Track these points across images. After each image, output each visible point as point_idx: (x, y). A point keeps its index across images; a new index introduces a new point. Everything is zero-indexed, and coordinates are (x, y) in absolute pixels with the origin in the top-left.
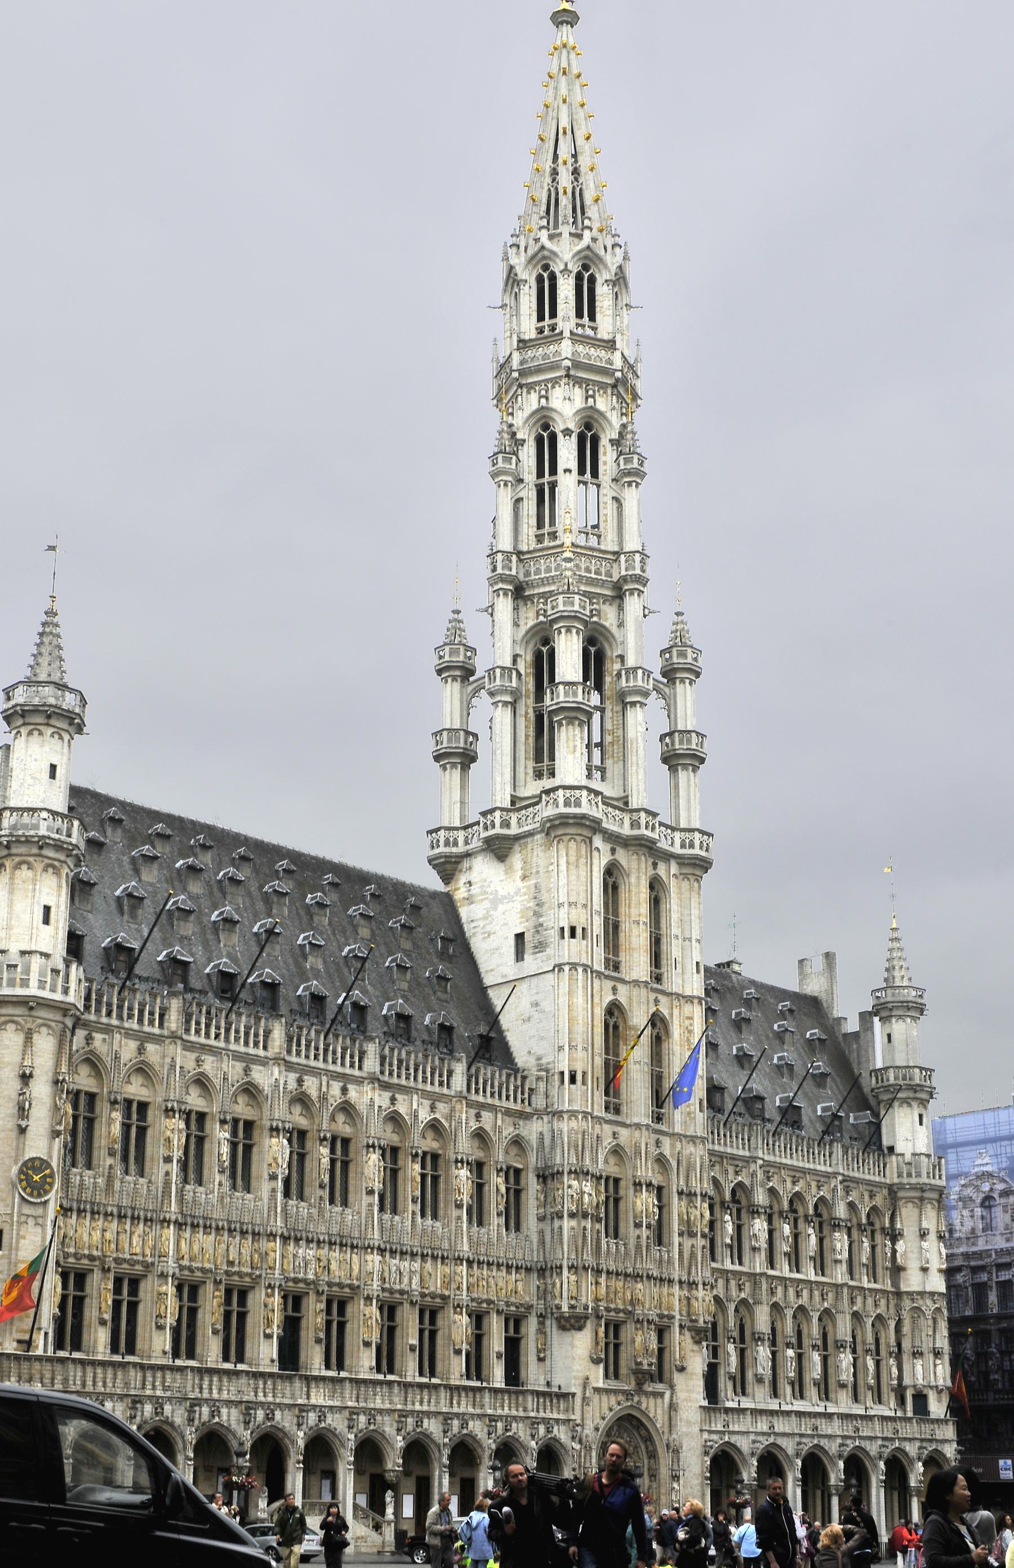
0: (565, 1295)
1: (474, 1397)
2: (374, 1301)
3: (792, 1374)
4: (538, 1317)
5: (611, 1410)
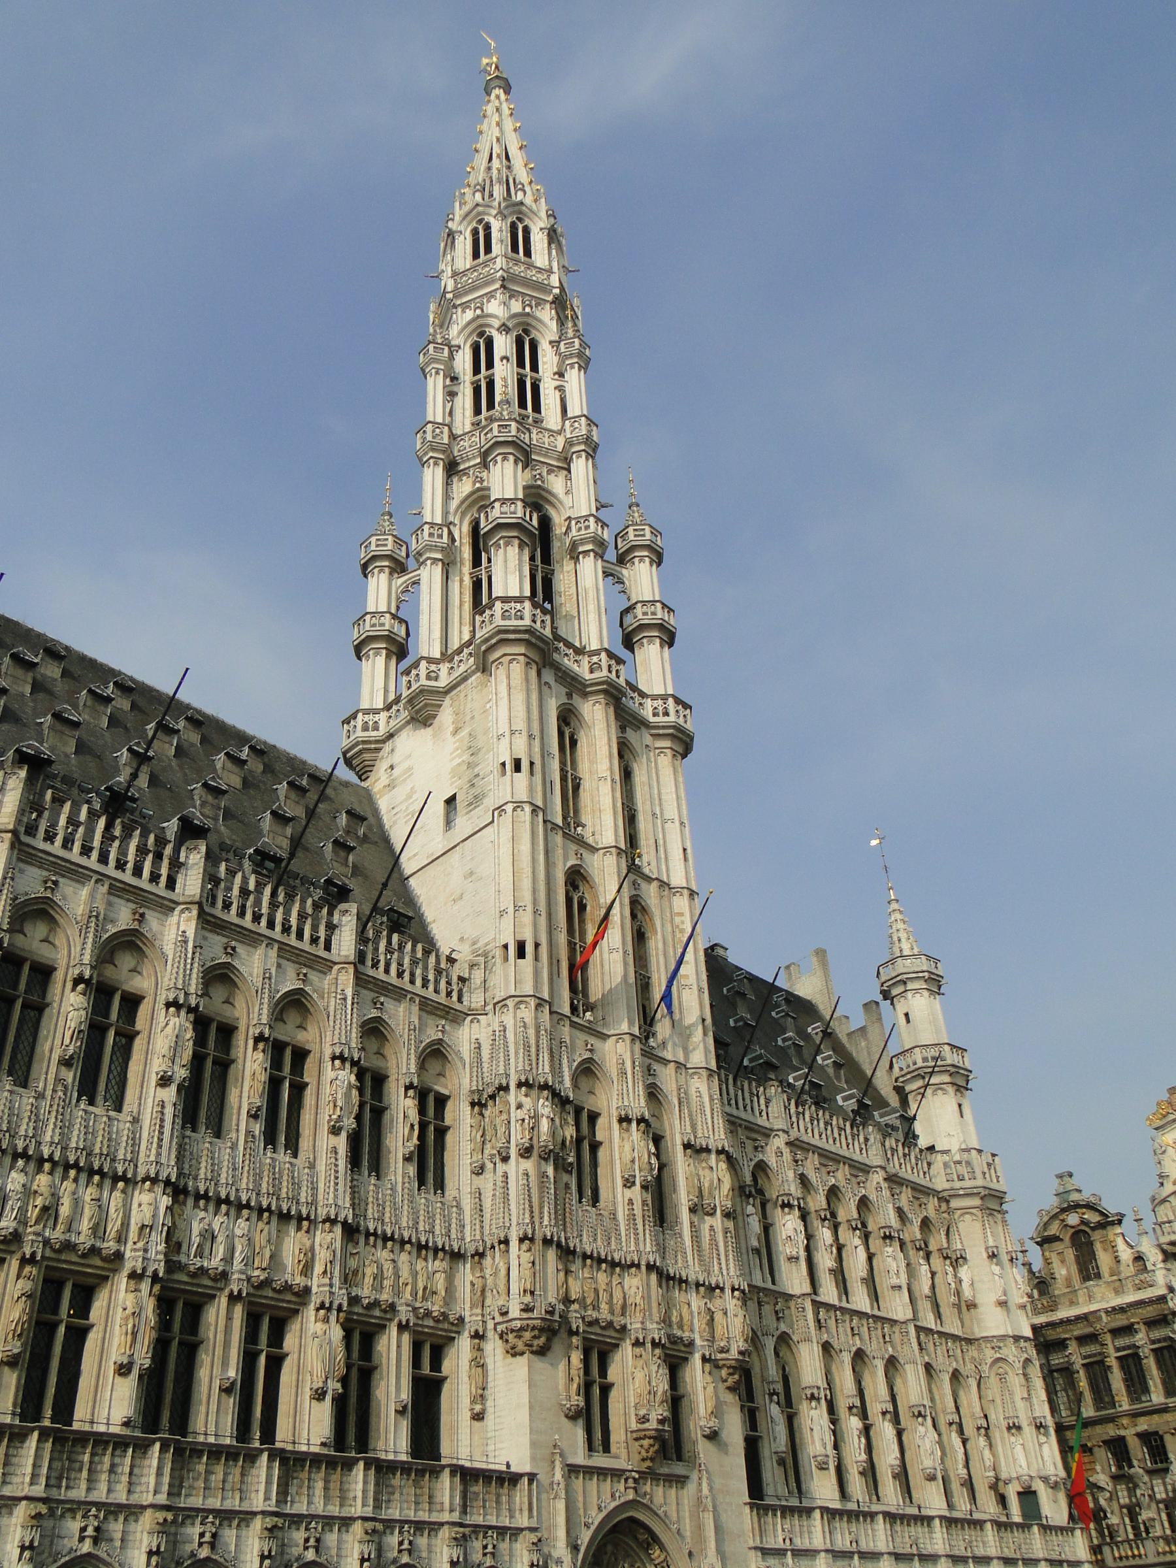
3: (864, 1457)
4: (472, 1337)
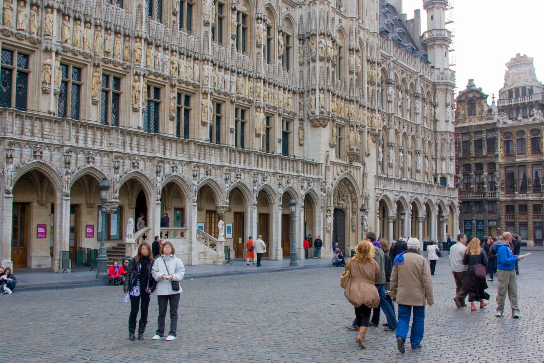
1: (270, 162)
2: (209, 96)
5: (338, 175)
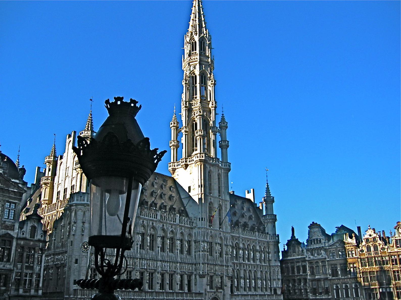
0: (201, 270)
3: (248, 286)
5: (211, 296)
